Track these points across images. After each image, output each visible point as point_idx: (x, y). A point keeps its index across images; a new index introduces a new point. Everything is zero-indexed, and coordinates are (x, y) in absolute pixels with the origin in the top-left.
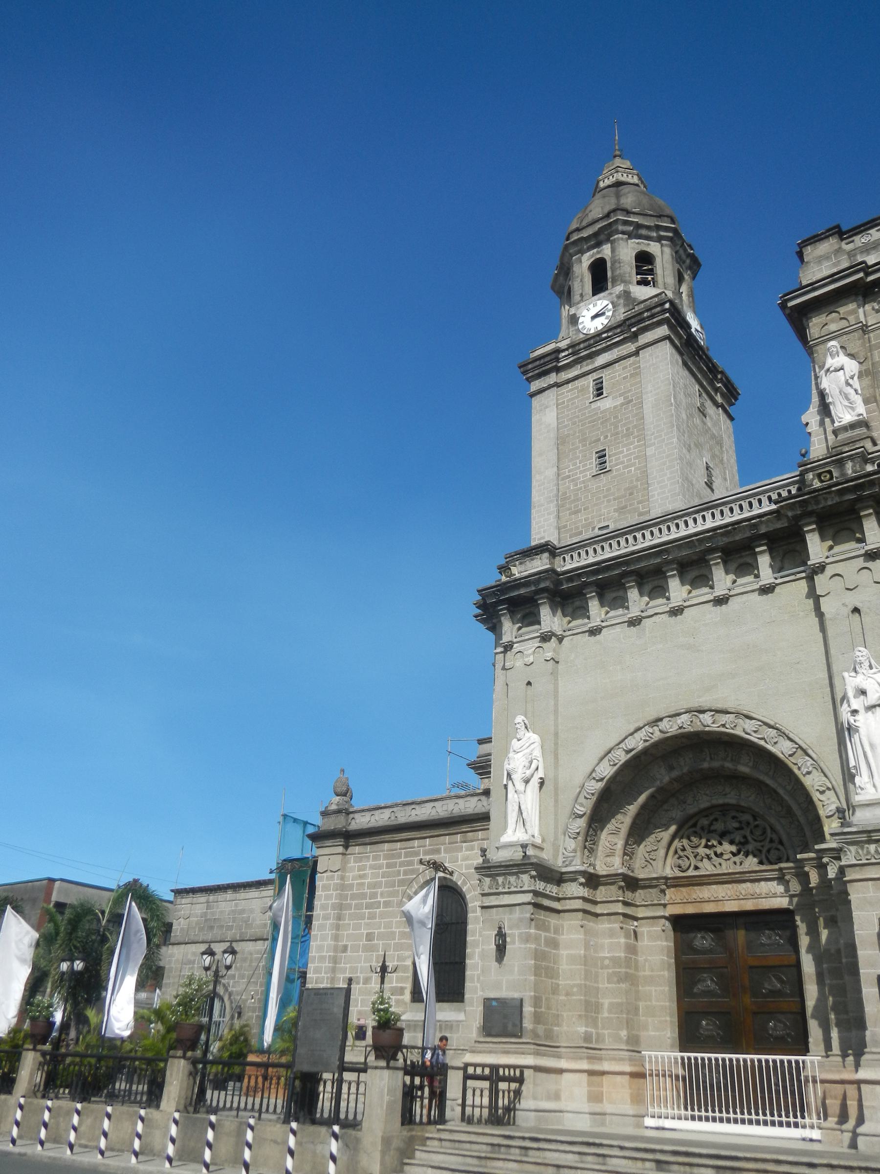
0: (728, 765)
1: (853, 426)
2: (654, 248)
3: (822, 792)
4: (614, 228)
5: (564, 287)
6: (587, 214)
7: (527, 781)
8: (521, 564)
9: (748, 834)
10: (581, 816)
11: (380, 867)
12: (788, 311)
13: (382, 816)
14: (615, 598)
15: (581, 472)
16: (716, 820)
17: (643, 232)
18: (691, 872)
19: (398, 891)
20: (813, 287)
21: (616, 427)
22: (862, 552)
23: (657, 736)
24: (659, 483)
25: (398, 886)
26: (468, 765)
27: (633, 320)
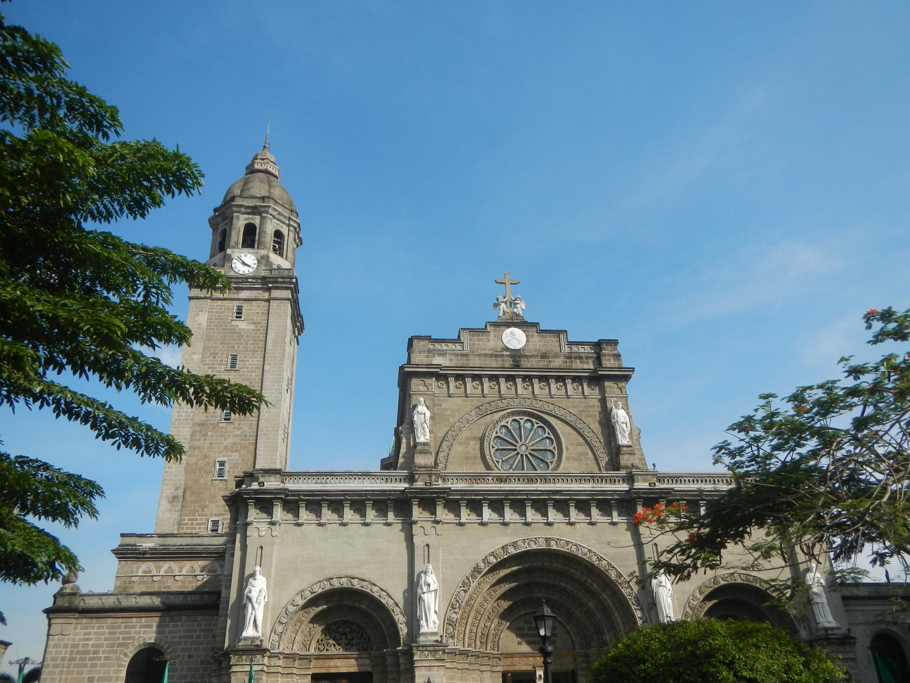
0: (357, 604)
1: (425, 444)
2: (284, 230)
3: (401, 624)
4: (266, 209)
5: (218, 225)
6: (249, 189)
7: (259, 604)
8: (262, 476)
9: (355, 635)
10: (283, 623)
11: (103, 634)
12: (403, 372)
13: (108, 600)
14: (312, 509)
15: (218, 364)
16: (340, 627)
17: (282, 218)
18: (324, 652)
19: (117, 650)
20: (417, 366)
21: (247, 344)
22: (433, 519)
23: (328, 587)
24: (269, 389)
25: (117, 647)
26: (112, 551)
27: (271, 280)
